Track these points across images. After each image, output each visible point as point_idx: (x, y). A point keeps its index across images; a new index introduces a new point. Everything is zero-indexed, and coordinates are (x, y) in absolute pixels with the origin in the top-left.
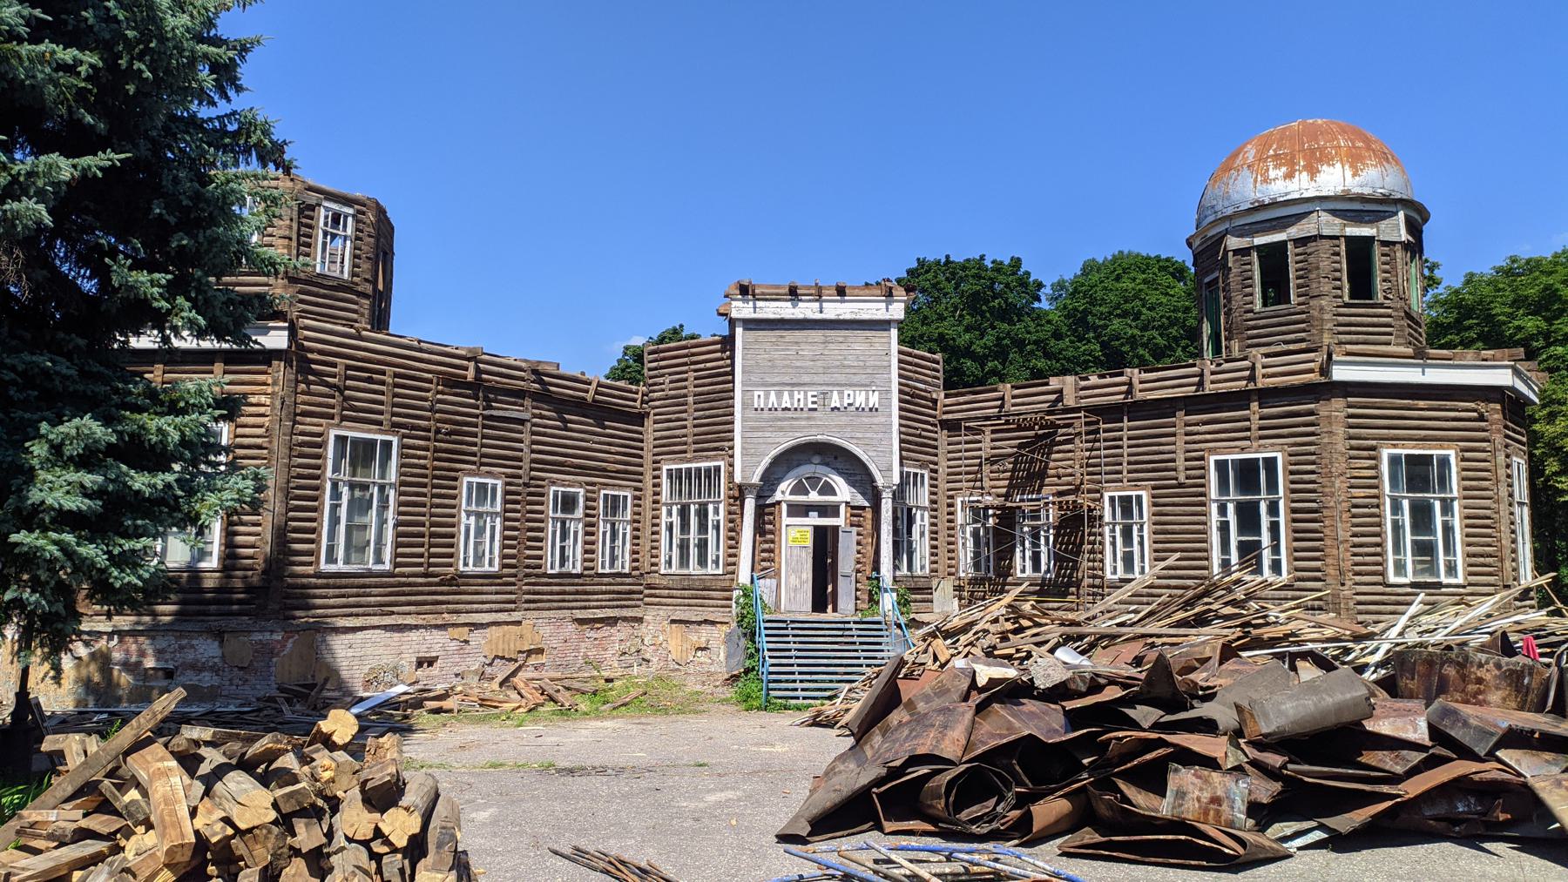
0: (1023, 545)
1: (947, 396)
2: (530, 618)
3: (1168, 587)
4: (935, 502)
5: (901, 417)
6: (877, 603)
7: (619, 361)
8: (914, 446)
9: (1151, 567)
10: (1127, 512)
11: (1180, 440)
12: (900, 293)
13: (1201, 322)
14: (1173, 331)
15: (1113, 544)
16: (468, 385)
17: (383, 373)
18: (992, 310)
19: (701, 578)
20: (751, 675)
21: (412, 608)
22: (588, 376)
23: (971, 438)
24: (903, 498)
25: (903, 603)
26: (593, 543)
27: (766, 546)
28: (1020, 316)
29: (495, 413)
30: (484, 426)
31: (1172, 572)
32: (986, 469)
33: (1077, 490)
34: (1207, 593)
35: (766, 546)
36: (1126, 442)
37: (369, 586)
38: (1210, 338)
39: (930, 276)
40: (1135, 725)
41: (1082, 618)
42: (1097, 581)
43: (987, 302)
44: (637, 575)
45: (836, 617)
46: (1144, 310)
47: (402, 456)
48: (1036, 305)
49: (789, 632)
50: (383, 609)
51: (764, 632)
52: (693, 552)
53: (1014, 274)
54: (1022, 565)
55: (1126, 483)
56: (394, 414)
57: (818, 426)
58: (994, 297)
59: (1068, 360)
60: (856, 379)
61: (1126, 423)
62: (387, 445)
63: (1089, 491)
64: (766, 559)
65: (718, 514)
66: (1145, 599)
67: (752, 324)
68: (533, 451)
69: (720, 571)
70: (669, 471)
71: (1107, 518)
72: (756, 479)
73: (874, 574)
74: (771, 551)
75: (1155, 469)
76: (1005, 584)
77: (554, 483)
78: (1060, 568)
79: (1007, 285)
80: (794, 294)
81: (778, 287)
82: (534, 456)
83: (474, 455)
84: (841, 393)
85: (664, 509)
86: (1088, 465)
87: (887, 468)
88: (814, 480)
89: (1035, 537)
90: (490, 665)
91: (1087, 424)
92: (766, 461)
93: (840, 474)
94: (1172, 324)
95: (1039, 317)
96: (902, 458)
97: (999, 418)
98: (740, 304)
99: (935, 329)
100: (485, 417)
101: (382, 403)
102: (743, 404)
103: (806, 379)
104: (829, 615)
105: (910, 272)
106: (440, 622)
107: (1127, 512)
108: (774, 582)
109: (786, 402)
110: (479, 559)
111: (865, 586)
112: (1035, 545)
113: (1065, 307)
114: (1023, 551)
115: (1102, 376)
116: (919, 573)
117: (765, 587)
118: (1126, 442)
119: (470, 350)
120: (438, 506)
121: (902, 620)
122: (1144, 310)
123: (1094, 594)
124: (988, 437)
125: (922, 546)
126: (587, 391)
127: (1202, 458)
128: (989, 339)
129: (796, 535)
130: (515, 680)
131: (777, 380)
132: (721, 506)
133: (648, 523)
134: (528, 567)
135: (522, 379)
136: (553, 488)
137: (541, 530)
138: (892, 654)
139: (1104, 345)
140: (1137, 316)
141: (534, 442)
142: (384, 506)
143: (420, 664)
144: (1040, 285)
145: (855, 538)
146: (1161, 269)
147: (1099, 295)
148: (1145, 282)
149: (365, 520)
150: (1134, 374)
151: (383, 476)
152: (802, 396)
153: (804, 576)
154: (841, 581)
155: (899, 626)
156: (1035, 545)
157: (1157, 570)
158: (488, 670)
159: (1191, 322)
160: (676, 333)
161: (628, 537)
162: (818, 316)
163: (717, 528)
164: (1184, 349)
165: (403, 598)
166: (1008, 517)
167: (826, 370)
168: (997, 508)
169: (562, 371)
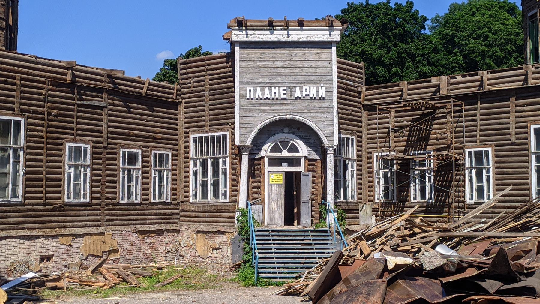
0: (415, 182)
1: (367, 89)
2: (109, 231)
3: (505, 207)
4: (360, 156)
5: (339, 103)
6: (325, 219)
7: (161, 69)
8: (347, 121)
9: (494, 195)
10: (479, 161)
11: (513, 116)
12: (338, 26)
13: (526, 41)
14: (508, 48)
15: (471, 181)
16: (68, 85)
17: (14, 78)
18: (394, 35)
19: (215, 205)
20: (248, 265)
21: (36, 225)
22: (143, 79)
23: (382, 115)
24: (340, 154)
25: (341, 219)
26: (148, 184)
27: (256, 184)
28: (412, 38)
29: (85, 102)
30: (78, 111)
31: (507, 198)
32: (392, 135)
33: (448, 147)
34: (529, 211)
35: (256, 184)
36: (479, 117)
37: (9, 212)
38: (531, 51)
39: (356, 13)
40: (485, 292)
41: (452, 227)
42: (461, 204)
43: (391, 30)
44: (175, 203)
45: (300, 228)
46: (490, 34)
47: (27, 130)
48: (423, 31)
49: (271, 237)
50: (18, 226)
51: (255, 238)
52: (210, 189)
53: (408, 12)
54: (414, 195)
55: (479, 143)
56: (21, 104)
57: (287, 109)
58: (396, 27)
59: (443, 66)
60: (311, 79)
61: (479, 106)
62: (18, 123)
63: (456, 148)
64: (255, 194)
65: (225, 165)
66: (490, 215)
67: (245, 45)
68: (109, 127)
69: (227, 201)
70: (195, 138)
71: (467, 165)
72: (249, 143)
73: (323, 201)
74: (259, 187)
75: (497, 135)
76: (404, 207)
77: (122, 147)
78: (438, 196)
79: (404, 19)
80: (271, 26)
81: (261, 21)
82: (110, 129)
83: (72, 129)
84: (301, 88)
85: (192, 162)
86: (455, 132)
87: (330, 133)
88: (285, 144)
89: (423, 177)
90: (86, 260)
91: (454, 106)
92: (255, 131)
93: (301, 139)
94: (507, 44)
95: (424, 39)
96: (340, 129)
97: (400, 103)
98: (237, 32)
99: (359, 48)
100: (79, 105)
101: (13, 97)
102: (240, 95)
103: (279, 79)
104: (295, 227)
105: (344, 11)
106: (53, 234)
107: (479, 161)
108: (261, 207)
109: (267, 94)
110: (77, 194)
111: (317, 208)
112: (423, 182)
113: (440, 33)
114: (415, 186)
115: (464, 76)
116: (350, 200)
117: (255, 210)
118: (479, 117)
119: (68, 63)
120: (51, 161)
121: (341, 230)
122: (490, 34)
123: (459, 212)
124: (393, 114)
125: (352, 184)
126: (142, 88)
127: (526, 127)
128: (393, 54)
129: (274, 178)
130: (102, 269)
131: (261, 80)
132: (227, 160)
133: (182, 171)
134: (108, 199)
135: (101, 81)
136: (122, 150)
137: (115, 176)
138: (334, 250)
139: (465, 57)
140: (486, 39)
141: (110, 121)
142: (17, 162)
143: (42, 259)
144: (425, 19)
145: (311, 179)
146: (501, 7)
147: (462, 25)
148: (491, 16)
149: (5, 171)
150: (484, 74)
151: (16, 143)
152: (277, 90)
153: (280, 203)
154: (303, 207)
155: (339, 233)
156: (423, 182)
157: (497, 197)
158: (85, 263)
159: (520, 42)
160: (196, 51)
161: (170, 180)
162: (287, 39)
163: (225, 173)
164: (515, 59)
165: (30, 219)
166: (406, 165)
167: (292, 74)
168: (399, 159)
169: (127, 75)
